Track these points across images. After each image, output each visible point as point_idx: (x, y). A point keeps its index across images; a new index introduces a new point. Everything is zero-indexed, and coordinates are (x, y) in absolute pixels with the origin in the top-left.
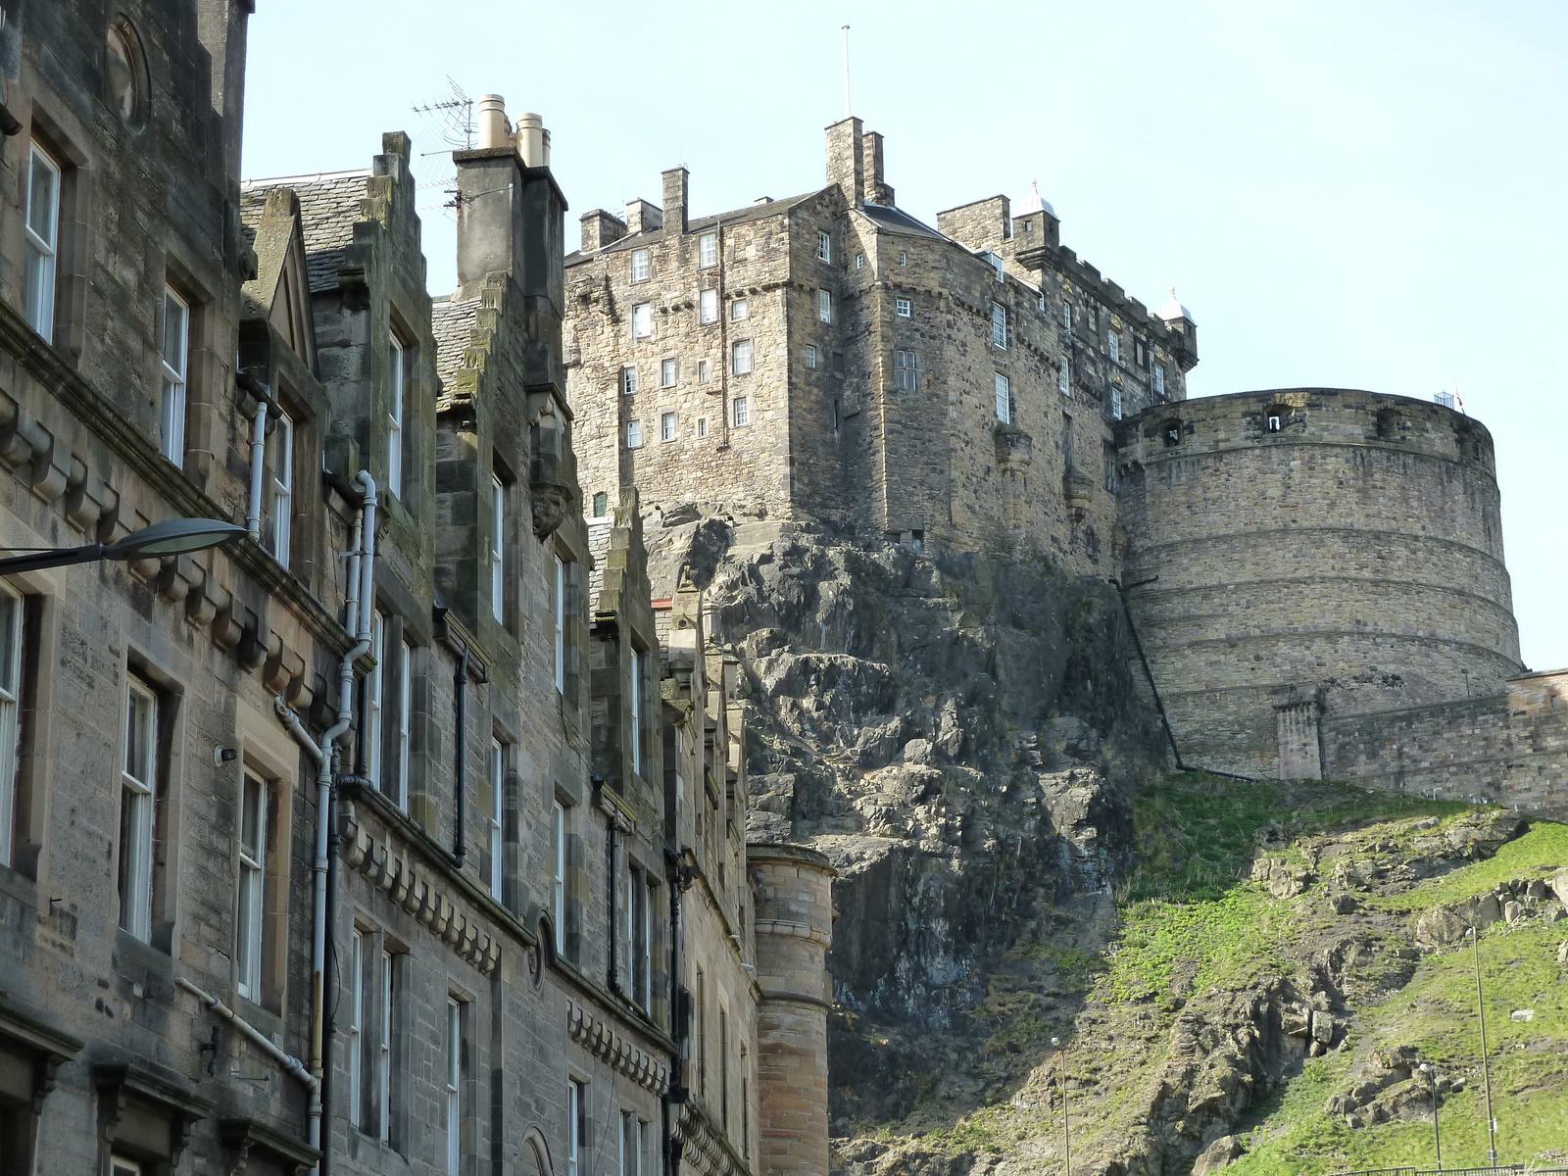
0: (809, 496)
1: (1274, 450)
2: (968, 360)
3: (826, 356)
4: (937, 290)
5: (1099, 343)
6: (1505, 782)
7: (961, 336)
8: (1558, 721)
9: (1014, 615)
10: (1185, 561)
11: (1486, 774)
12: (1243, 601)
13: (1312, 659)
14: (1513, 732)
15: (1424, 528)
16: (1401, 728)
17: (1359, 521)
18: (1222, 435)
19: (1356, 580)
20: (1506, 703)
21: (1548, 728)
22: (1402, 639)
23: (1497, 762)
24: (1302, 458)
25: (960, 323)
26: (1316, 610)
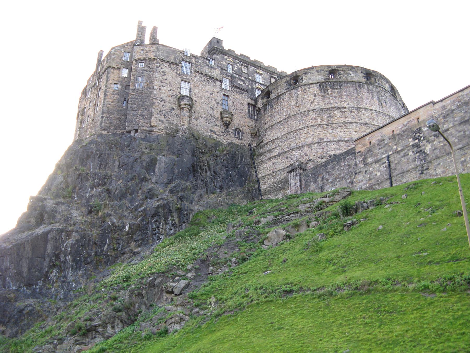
0: (108, 127)
1: (293, 90)
2: (166, 77)
3: (122, 86)
4: (152, 57)
5: (249, 76)
6: (355, 180)
7: (162, 70)
8: (372, 151)
9: (172, 152)
10: (269, 133)
11: (348, 179)
12: (283, 141)
13: (303, 154)
14: (357, 160)
15: (348, 104)
16: (323, 169)
17: (322, 106)
18: (279, 91)
19: (320, 125)
20: (355, 150)
21: (369, 155)
22: (338, 142)
23: (352, 173)
24: (301, 90)
25: (162, 66)
26: (305, 137)
